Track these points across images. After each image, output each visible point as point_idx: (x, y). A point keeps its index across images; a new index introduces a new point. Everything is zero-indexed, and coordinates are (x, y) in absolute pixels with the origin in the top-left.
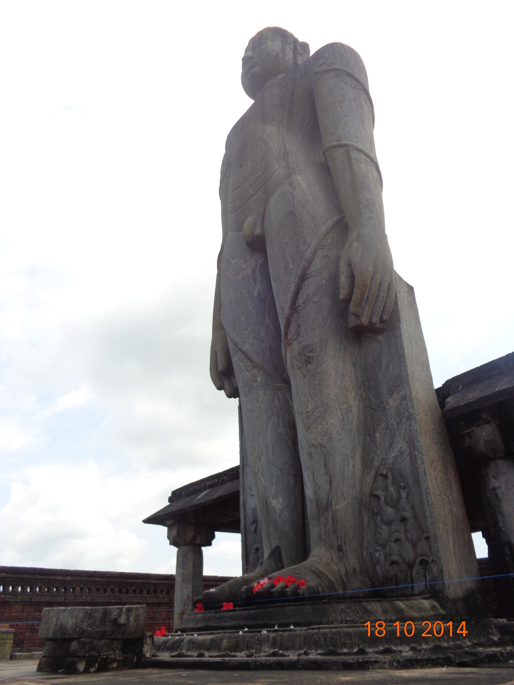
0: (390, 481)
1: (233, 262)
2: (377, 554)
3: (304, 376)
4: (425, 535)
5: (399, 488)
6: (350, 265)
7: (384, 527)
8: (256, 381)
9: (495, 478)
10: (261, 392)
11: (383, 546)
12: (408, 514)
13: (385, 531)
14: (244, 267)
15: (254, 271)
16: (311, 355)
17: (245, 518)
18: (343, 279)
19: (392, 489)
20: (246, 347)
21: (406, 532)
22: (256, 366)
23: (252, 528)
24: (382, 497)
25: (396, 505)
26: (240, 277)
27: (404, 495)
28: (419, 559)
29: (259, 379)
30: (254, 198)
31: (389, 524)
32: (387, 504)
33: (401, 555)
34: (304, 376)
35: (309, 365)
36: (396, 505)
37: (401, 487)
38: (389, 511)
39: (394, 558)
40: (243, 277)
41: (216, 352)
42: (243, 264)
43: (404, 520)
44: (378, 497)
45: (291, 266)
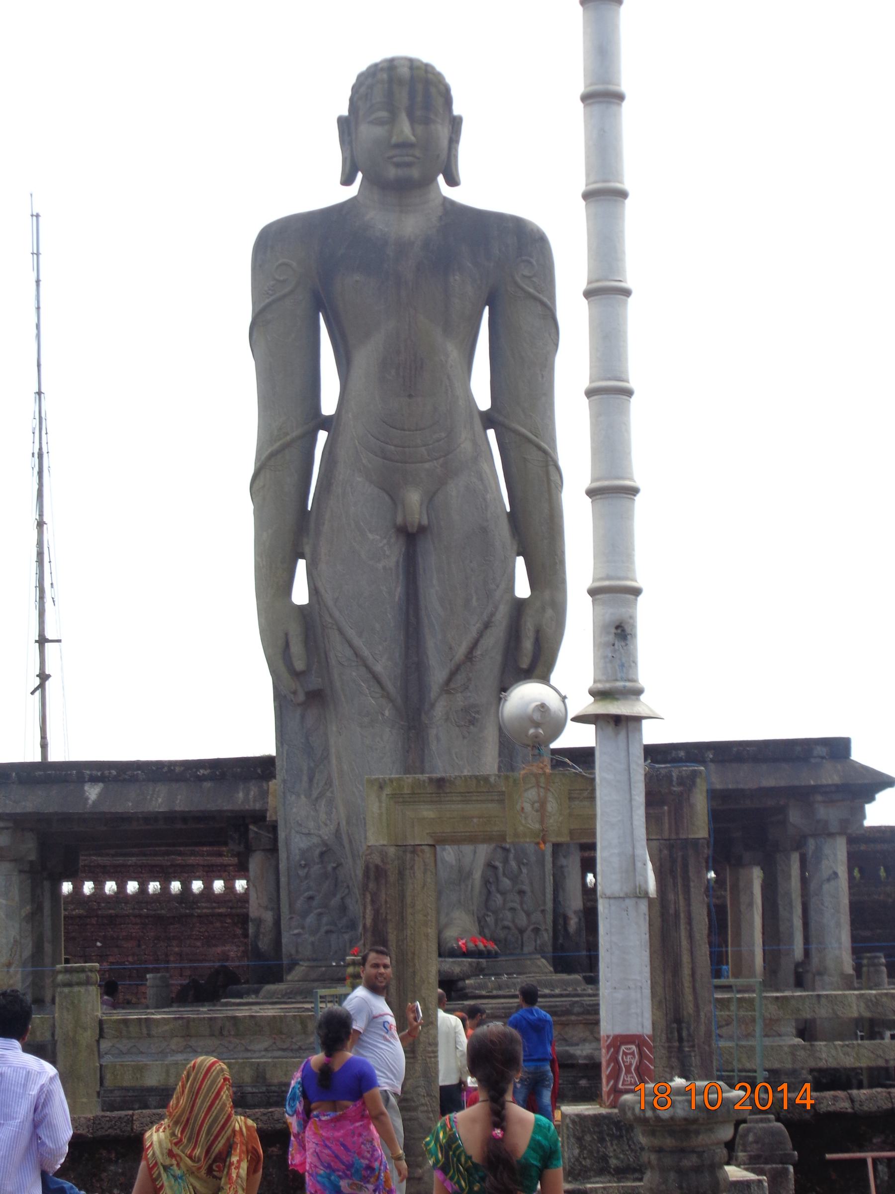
0: (511, 856)
1: (370, 536)
2: (488, 919)
3: (464, 737)
4: (542, 908)
5: (520, 863)
6: (538, 631)
7: (499, 896)
8: (383, 715)
9: (565, 857)
10: (388, 730)
11: (495, 912)
12: (526, 888)
13: (498, 899)
14: (387, 553)
15: (397, 562)
16: (477, 716)
17: (288, 858)
18: (528, 645)
19: (513, 864)
20: (378, 668)
21: (521, 904)
22: (388, 697)
23: (302, 873)
24: (501, 870)
25: (515, 879)
26: (380, 566)
27: (524, 870)
28: (532, 927)
29: (387, 713)
30: (427, 465)
31: (503, 894)
32: (504, 874)
33: (513, 921)
34: (464, 737)
35: (472, 727)
36: (515, 879)
37: (523, 864)
38: (506, 883)
39: (506, 923)
40: (384, 568)
41: (286, 635)
42: (386, 548)
43: (521, 893)
44: (495, 868)
45: (474, 603)
